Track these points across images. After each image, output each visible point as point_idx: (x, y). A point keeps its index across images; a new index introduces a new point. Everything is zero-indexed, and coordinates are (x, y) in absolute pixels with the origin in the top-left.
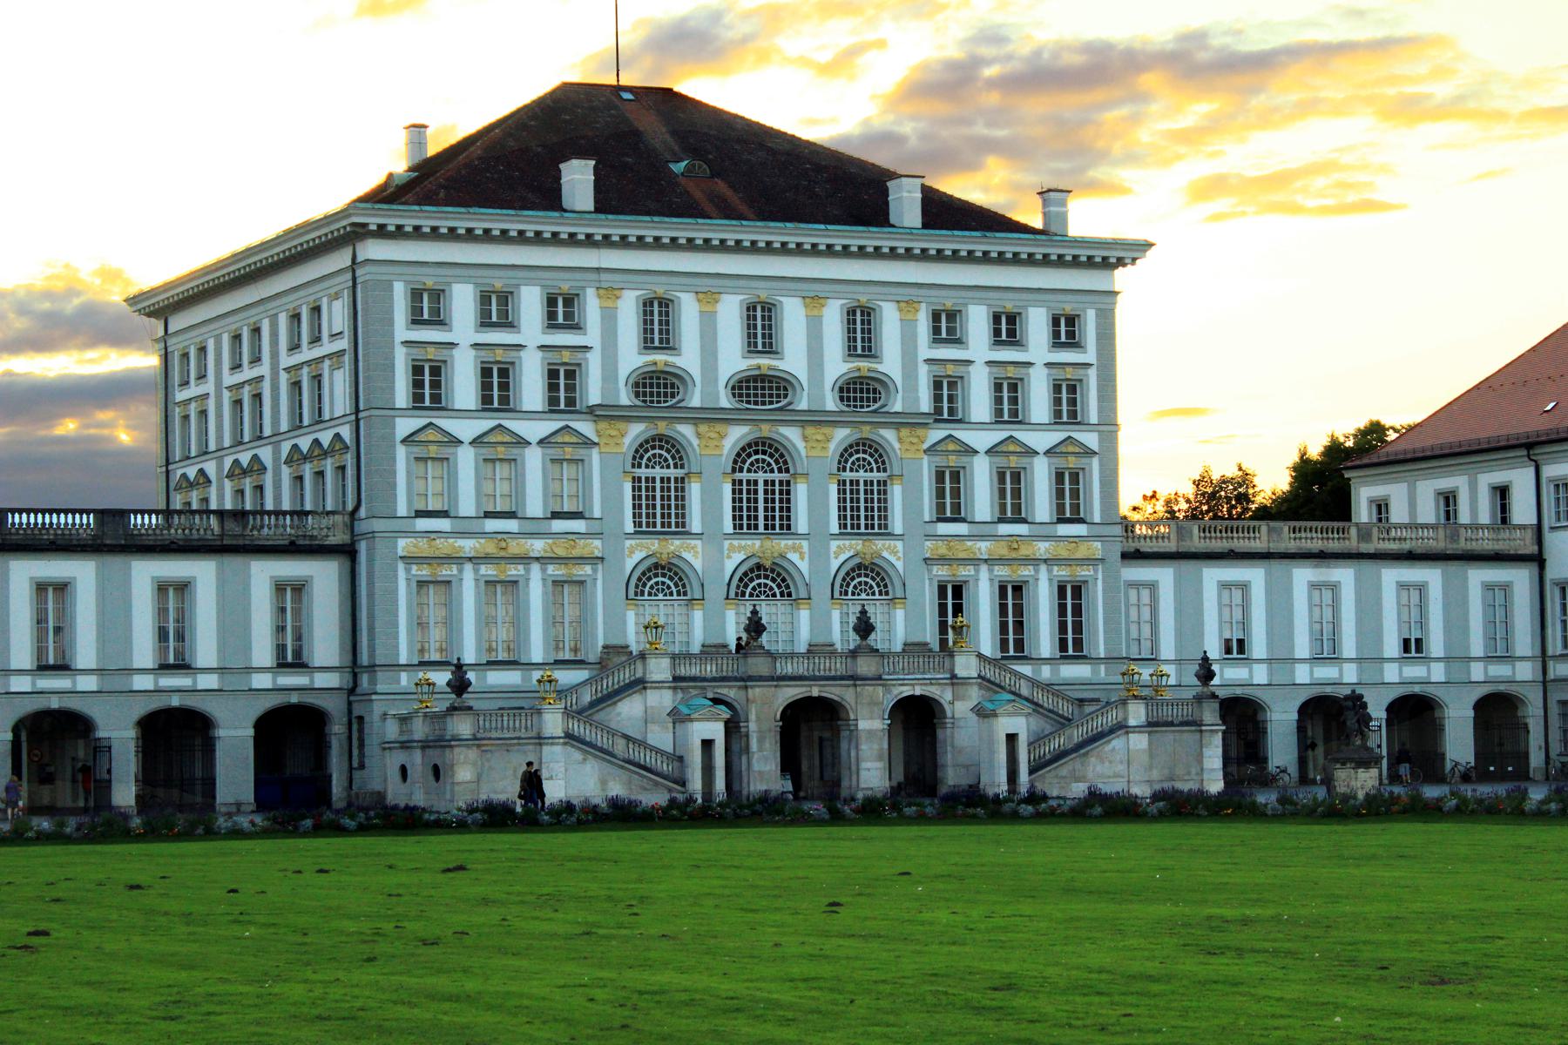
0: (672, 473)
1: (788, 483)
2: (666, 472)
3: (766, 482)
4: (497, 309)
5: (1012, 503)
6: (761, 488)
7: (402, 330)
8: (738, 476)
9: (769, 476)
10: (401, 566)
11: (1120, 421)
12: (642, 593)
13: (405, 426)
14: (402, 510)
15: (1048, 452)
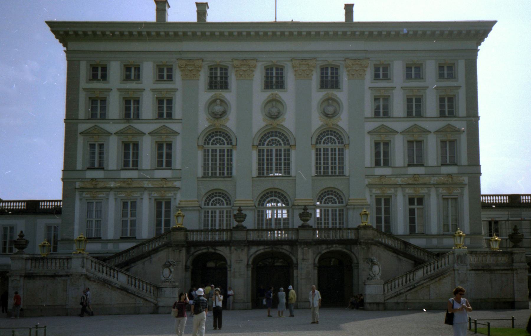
0: (226, 147)
1: (289, 150)
2: (222, 147)
3: (277, 150)
4: (132, 72)
5: (416, 156)
6: (274, 153)
7: (83, 84)
8: (261, 147)
9: (279, 147)
10: (77, 193)
11: (480, 114)
12: (208, 205)
13: (82, 127)
14: (79, 166)
15: (437, 132)
